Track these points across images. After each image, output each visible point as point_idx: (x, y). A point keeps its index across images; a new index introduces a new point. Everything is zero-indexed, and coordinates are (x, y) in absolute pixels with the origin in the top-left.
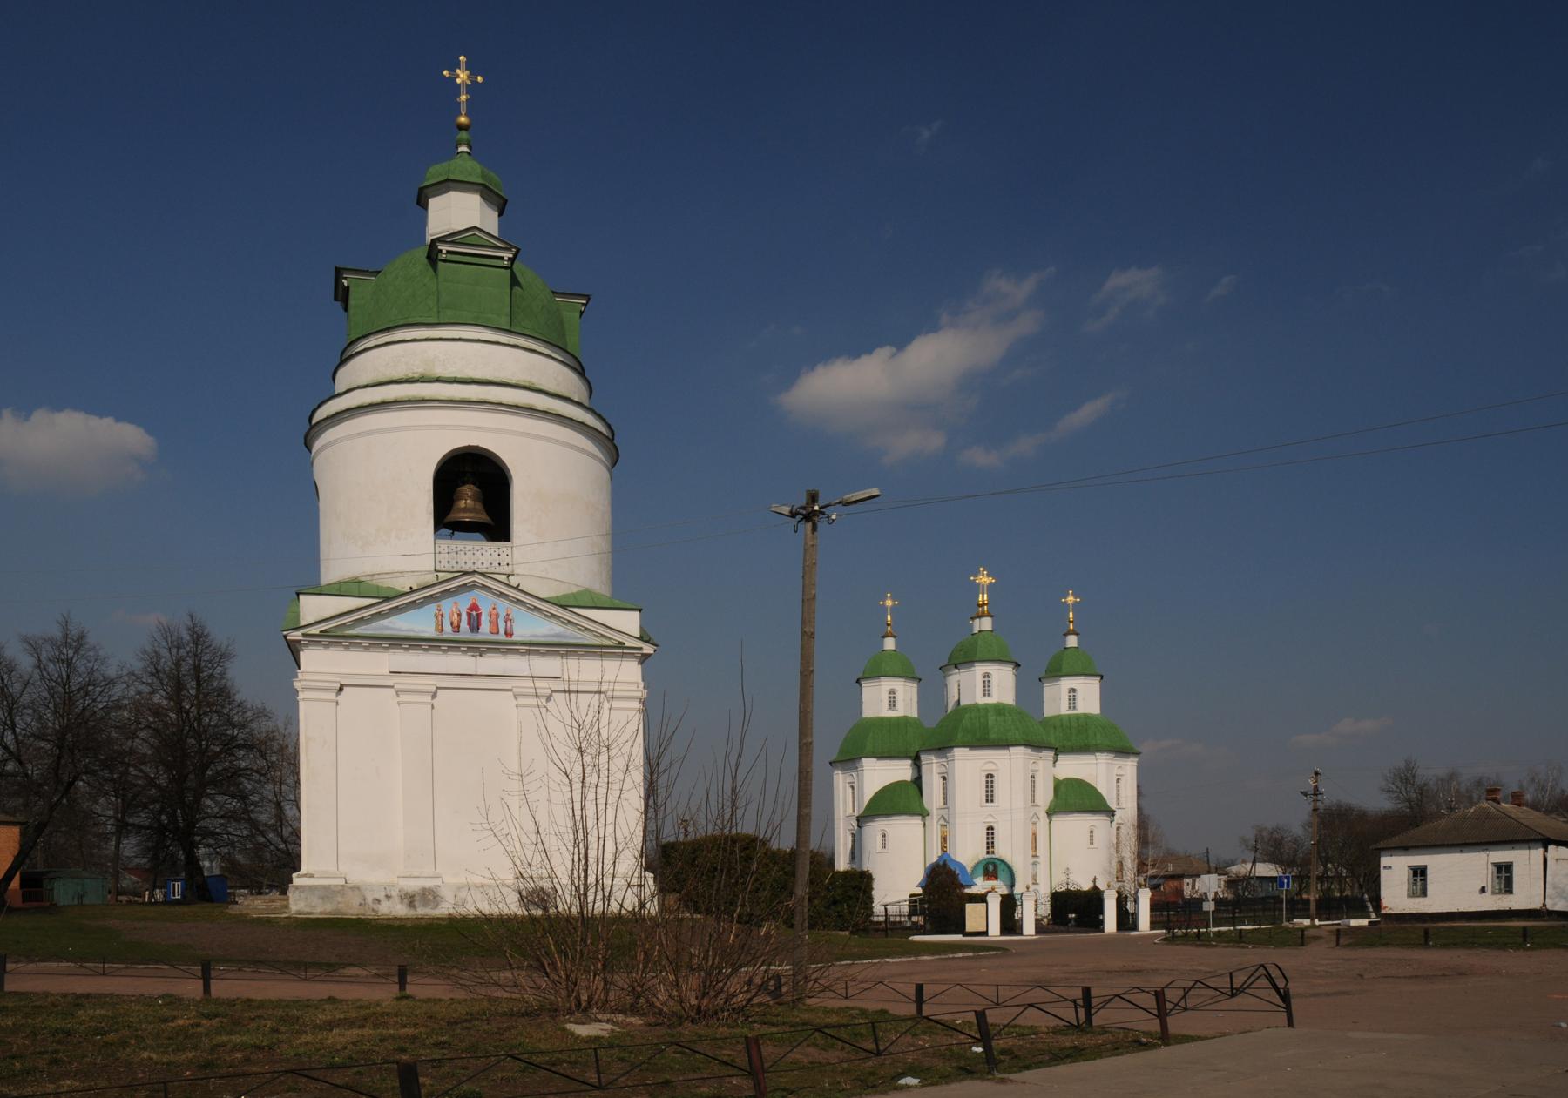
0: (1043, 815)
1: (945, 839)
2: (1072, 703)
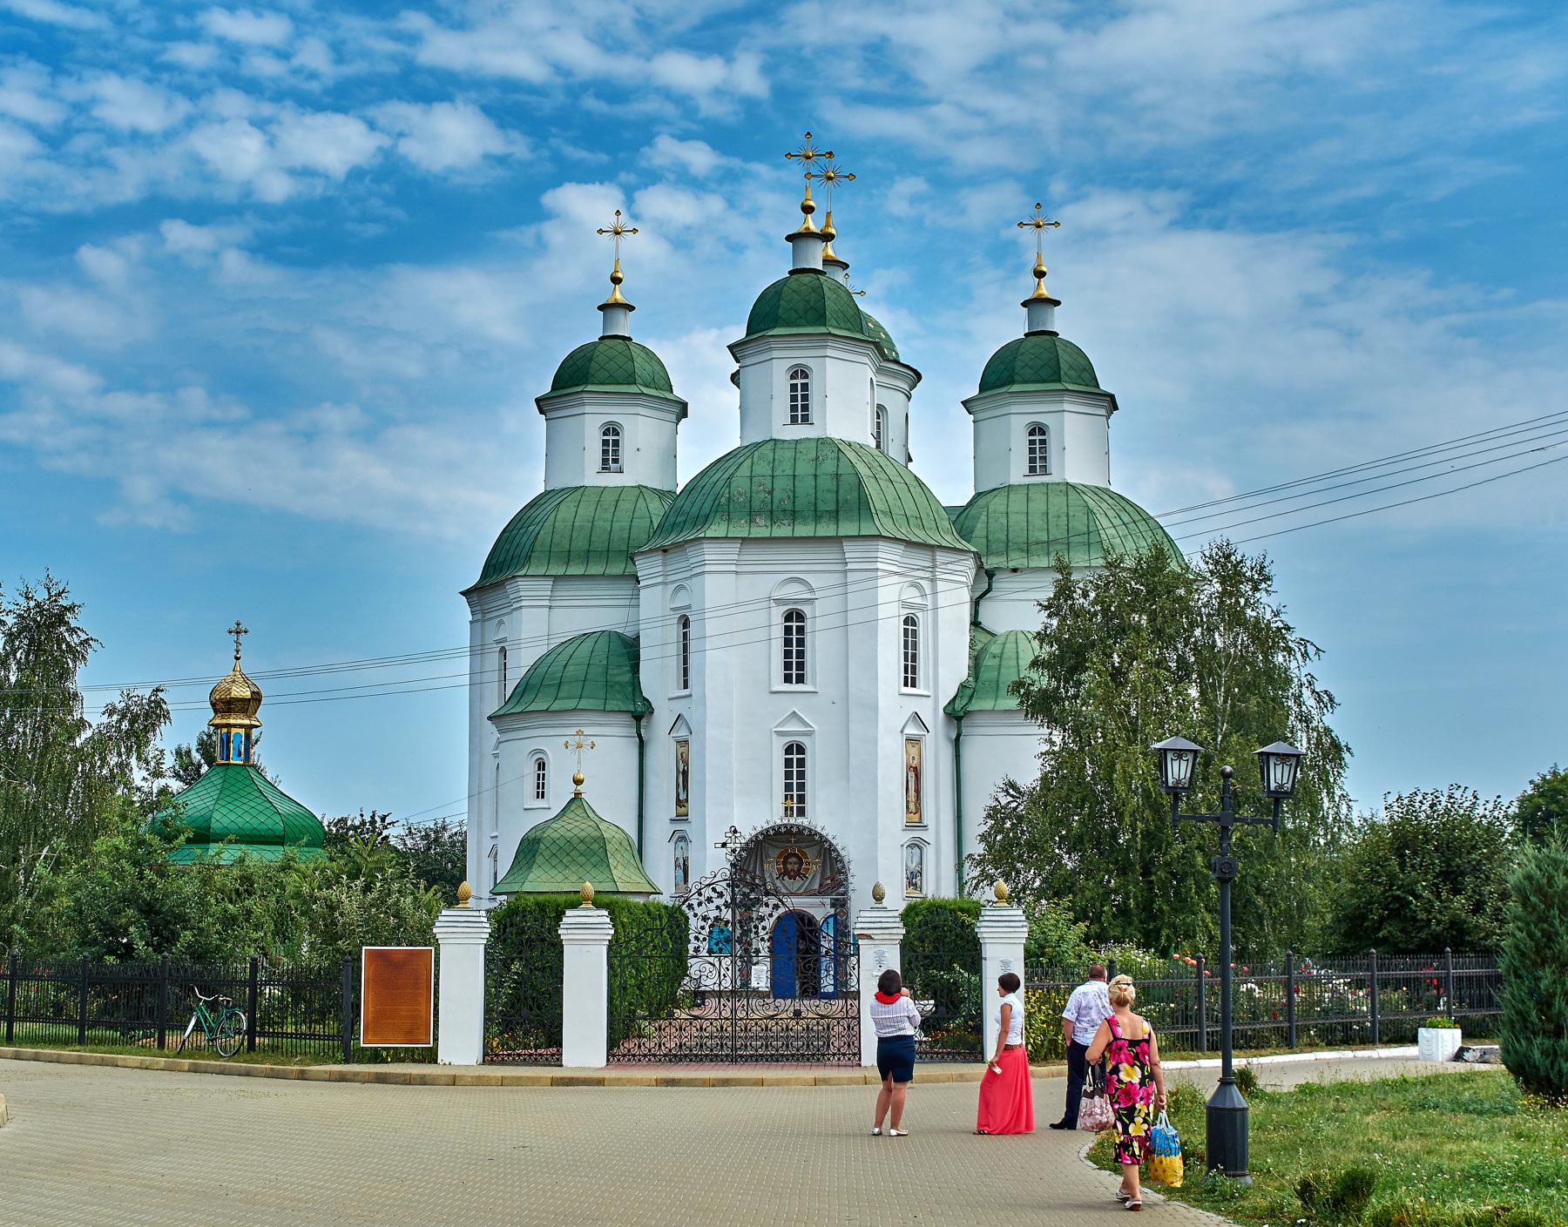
1: (684, 775)
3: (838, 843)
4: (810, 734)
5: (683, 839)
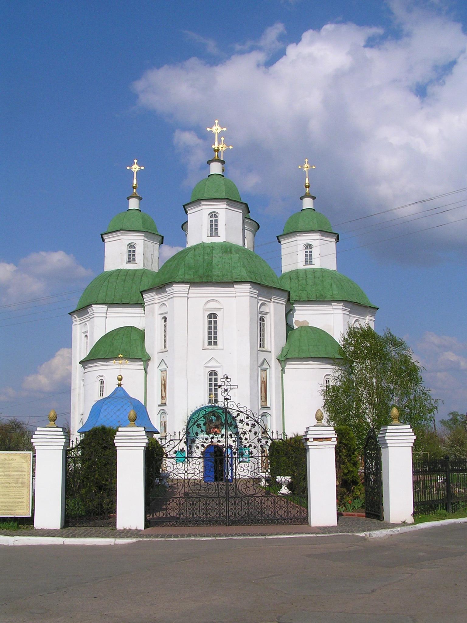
0: (274, 362)
1: (164, 386)
2: (309, 258)
4: (219, 367)
5: (164, 412)
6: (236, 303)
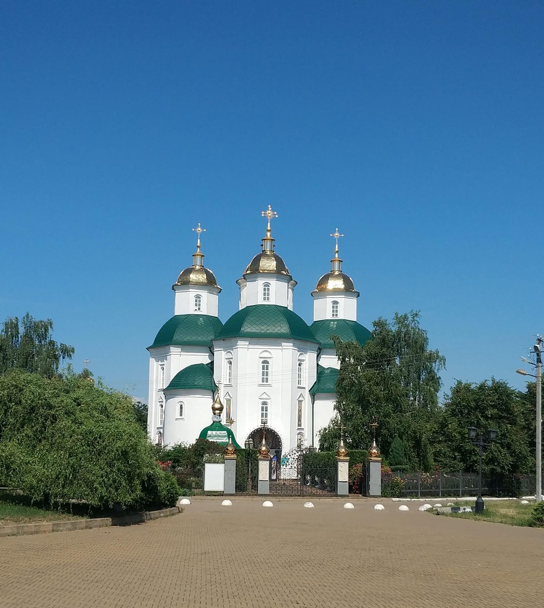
3: (280, 433)
6: (284, 355)
